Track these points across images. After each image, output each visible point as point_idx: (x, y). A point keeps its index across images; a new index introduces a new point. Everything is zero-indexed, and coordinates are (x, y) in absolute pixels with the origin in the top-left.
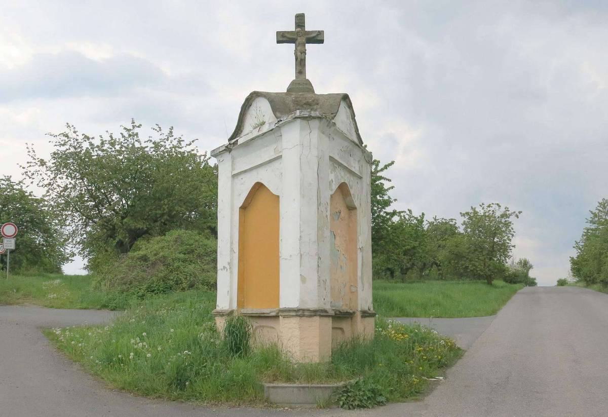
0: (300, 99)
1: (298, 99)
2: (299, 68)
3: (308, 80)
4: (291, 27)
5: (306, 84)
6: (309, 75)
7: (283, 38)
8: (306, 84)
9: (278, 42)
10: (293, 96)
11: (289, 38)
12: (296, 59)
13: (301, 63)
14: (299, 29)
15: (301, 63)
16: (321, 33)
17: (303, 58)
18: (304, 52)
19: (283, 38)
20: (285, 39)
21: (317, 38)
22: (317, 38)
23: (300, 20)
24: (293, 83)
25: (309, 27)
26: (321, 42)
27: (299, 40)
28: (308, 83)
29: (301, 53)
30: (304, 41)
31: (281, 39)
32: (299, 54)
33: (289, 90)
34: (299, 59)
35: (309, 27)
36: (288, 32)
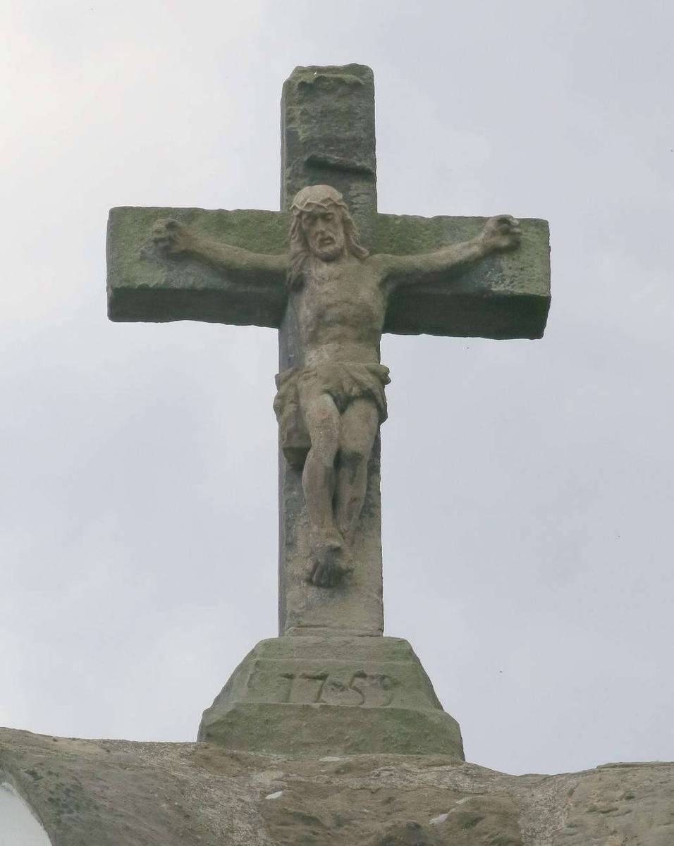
0: (338, 803)
1: (313, 806)
2: (318, 535)
3: (403, 651)
4: (237, 170)
5: (387, 682)
6: (420, 596)
7: (170, 270)
8: (387, 682)
9: (129, 303)
10: (265, 778)
11: (231, 272)
12: (294, 455)
13: (331, 488)
14: (316, 193)
15: (331, 488)
16: (518, 239)
17: (356, 443)
18: (370, 396)
19: (170, 270)
20: (188, 277)
21: (485, 288)
22: (485, 288)
23: (330, 120)
24: (258, 666)
25: (403, 189)
26: (524, 316)
27: (336, 286)
28: (402, 670)
29: (343, 403)
30: (368, 292)
31: (154, 276)
32: (319, 405)
33: (227, 729)
34: (319, 458)
35: (403, 189)
36: (221, 221)
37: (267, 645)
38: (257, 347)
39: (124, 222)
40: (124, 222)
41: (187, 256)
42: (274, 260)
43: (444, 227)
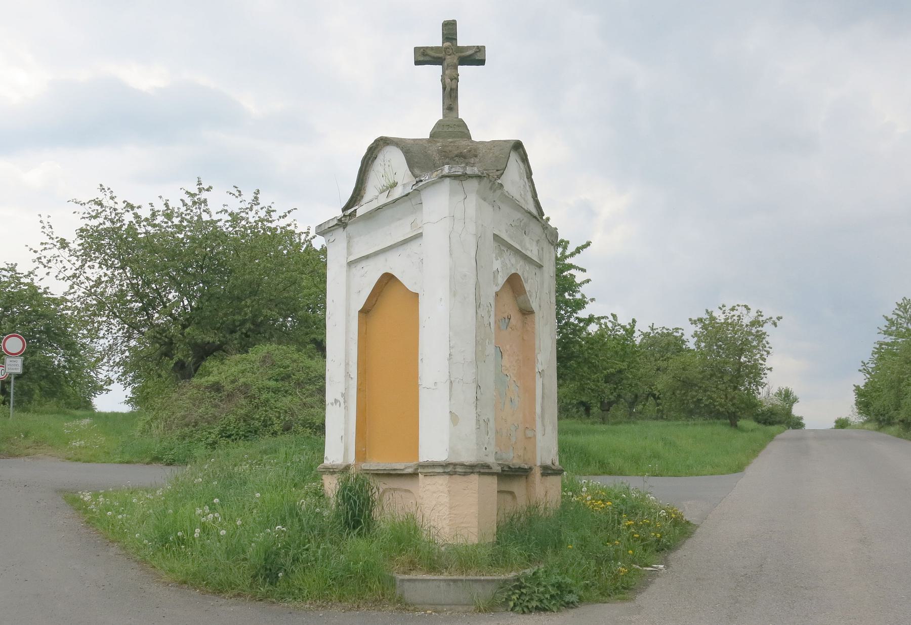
0: (450, 148)
1: (447, 149)
2: (448, 102)
3: (461, 120)
4: (436, 40)
5: (459, 126)
6: (464, 112)
7: (424, 57)
8: (459, 126)
9: (417, 63)
10: (439, 144)
11: (434, 57)
12: (444, 89)
13: (450, 95)
14: (447, 44)
15: (450, 95)
16: (480, 49)
17: (454, 87)
18: (455, 79)
19: (424, 57)
20: (427, 58)
21: (475, 57)
22: (475, 57)
23: (450, 29)
24: (439, 124)
25: (461, 42)
26: (482, 62)
27: (449, 60)
28: (462, 124)
29: (451, 80)
30: (456, 61)
31: (421, 58)
32: (448, 81)
33: (433, 135)
34: (448, 89)
35: (461, 42)
36: (432, 48)
37: (440, 121)
38: (438, 69)
39: (416, 49)
40: (416, 49)
41: (427, 55)
42: (441, 55)
43: (468, 48)
